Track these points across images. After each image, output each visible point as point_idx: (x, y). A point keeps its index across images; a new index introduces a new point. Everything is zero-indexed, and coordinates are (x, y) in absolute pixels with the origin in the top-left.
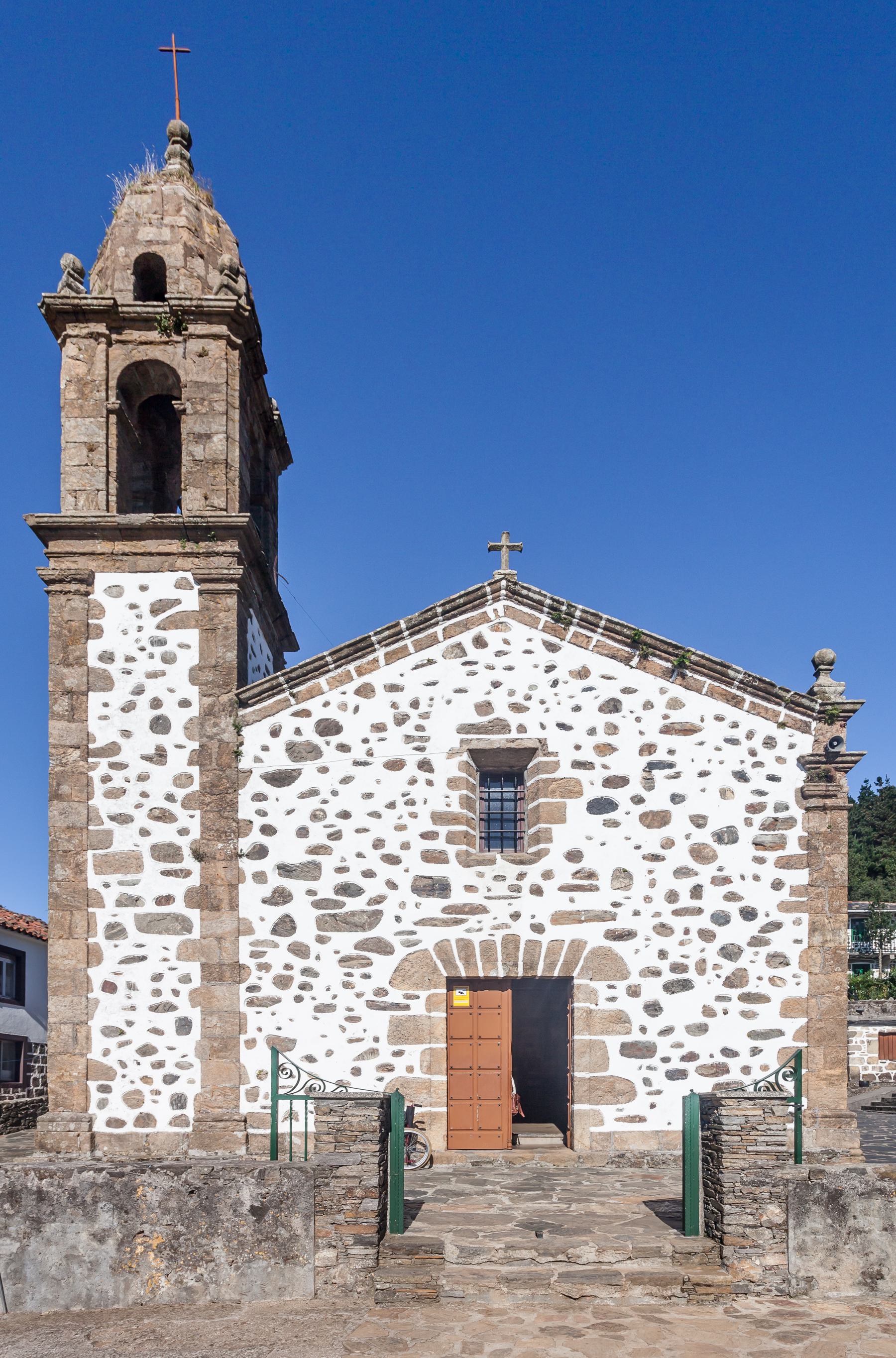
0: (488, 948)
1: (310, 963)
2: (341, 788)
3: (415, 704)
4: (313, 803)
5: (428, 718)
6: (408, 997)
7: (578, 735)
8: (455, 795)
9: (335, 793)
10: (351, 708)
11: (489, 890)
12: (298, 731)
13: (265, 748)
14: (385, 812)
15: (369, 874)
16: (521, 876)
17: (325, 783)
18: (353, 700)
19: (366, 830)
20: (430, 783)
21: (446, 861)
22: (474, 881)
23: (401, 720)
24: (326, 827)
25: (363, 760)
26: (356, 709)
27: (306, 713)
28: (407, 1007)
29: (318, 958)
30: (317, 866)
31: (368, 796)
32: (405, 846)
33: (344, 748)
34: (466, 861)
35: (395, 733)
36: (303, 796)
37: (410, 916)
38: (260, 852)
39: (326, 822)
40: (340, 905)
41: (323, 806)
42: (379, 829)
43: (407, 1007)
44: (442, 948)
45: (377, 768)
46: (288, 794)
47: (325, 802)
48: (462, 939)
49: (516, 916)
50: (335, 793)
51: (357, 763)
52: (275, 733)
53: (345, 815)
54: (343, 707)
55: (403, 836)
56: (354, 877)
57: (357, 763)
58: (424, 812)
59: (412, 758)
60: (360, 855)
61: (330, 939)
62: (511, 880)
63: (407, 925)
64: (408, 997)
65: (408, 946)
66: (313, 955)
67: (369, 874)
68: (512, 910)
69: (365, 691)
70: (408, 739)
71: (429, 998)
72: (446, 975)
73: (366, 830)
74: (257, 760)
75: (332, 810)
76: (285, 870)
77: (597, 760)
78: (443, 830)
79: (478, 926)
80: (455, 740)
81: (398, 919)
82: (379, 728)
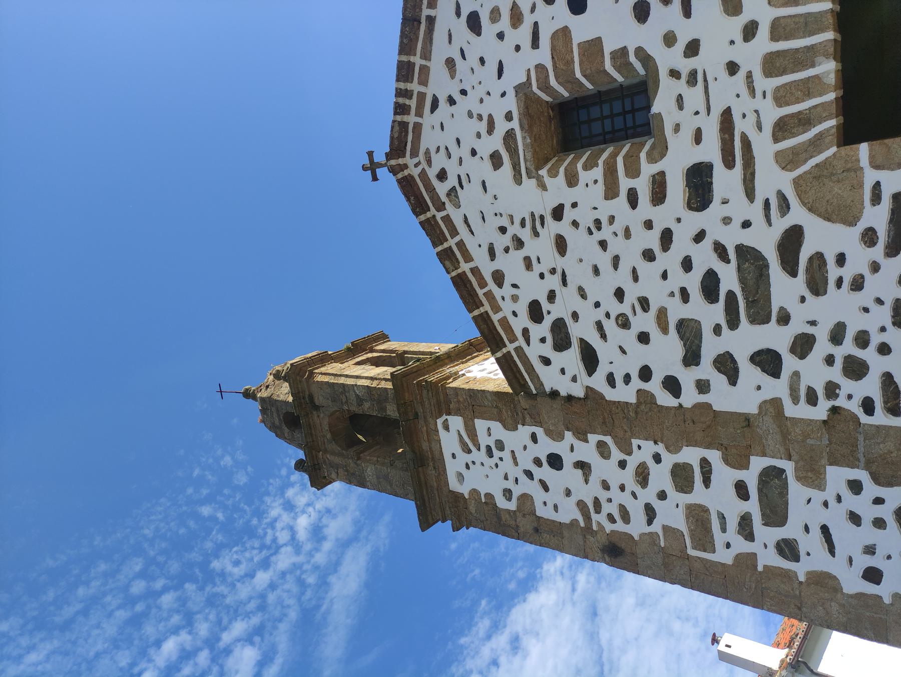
0: (781, 97)
1: (822, 334)
2: (591, 300)
3: (503, 230)
4: (610, 326)
5: (512, 216)
6: (876, 198)
7: (504, 51)
8: (584, 176)
9: (597, 305)
10: (515, 291)
11: (697, 113)
13: (563, 371)
14: (612, 250)
15: (687, 264)
16: (675, 74)
17: (590, 316)
18: (507, 290)
19: (634, 271)
20: (574, 205)
21: (662, 174)
22: (687, 134)
23: (519, 243)
24: (635, 314)
25: (560, 278)
26: (515, 286)
27: (526, 332)
29: (813, 323)
30: (682, 325)
31: (596, 271)
32: (649, 225)
33: (552, 296)
34: (660, 151)
35: (532, 248)
36: (604, 336)
37: (740, 208)
38: (672, 385)
39: (629, 313)
40: (731, 295)
41: (613, 316)
42: (631, 256)
44: (787, 161)
45: (565, 263)
47: (608, 315)
48: (774, 135)
49: (732, 68)
50: (597, 305)
51: (564, 282)
52: (546, 361)
53: (619, 294)
54: (515, 298)
55: (637, 229)
56: (693, 281)
57: (564, 282)
58: (607, 208)
60: (665, 276)
61: (782, 309)
62: (681, 86)
63: (755, 212)
64: (876, 198)
65: (788, 208)
66: (810, 330)
67: (687, 264)
68: (723, 74)
69: (498, 276)
70: (536, 234)
71: (876, 166)
72: (834, 149)
73: (634, 271)
74: (574, 379)
75: (616, 308)
76: (692, 358)
77: (528, 21)
78: (625, 183)
79: (752, 118)
80: (529, 184)
81: (746, 224)
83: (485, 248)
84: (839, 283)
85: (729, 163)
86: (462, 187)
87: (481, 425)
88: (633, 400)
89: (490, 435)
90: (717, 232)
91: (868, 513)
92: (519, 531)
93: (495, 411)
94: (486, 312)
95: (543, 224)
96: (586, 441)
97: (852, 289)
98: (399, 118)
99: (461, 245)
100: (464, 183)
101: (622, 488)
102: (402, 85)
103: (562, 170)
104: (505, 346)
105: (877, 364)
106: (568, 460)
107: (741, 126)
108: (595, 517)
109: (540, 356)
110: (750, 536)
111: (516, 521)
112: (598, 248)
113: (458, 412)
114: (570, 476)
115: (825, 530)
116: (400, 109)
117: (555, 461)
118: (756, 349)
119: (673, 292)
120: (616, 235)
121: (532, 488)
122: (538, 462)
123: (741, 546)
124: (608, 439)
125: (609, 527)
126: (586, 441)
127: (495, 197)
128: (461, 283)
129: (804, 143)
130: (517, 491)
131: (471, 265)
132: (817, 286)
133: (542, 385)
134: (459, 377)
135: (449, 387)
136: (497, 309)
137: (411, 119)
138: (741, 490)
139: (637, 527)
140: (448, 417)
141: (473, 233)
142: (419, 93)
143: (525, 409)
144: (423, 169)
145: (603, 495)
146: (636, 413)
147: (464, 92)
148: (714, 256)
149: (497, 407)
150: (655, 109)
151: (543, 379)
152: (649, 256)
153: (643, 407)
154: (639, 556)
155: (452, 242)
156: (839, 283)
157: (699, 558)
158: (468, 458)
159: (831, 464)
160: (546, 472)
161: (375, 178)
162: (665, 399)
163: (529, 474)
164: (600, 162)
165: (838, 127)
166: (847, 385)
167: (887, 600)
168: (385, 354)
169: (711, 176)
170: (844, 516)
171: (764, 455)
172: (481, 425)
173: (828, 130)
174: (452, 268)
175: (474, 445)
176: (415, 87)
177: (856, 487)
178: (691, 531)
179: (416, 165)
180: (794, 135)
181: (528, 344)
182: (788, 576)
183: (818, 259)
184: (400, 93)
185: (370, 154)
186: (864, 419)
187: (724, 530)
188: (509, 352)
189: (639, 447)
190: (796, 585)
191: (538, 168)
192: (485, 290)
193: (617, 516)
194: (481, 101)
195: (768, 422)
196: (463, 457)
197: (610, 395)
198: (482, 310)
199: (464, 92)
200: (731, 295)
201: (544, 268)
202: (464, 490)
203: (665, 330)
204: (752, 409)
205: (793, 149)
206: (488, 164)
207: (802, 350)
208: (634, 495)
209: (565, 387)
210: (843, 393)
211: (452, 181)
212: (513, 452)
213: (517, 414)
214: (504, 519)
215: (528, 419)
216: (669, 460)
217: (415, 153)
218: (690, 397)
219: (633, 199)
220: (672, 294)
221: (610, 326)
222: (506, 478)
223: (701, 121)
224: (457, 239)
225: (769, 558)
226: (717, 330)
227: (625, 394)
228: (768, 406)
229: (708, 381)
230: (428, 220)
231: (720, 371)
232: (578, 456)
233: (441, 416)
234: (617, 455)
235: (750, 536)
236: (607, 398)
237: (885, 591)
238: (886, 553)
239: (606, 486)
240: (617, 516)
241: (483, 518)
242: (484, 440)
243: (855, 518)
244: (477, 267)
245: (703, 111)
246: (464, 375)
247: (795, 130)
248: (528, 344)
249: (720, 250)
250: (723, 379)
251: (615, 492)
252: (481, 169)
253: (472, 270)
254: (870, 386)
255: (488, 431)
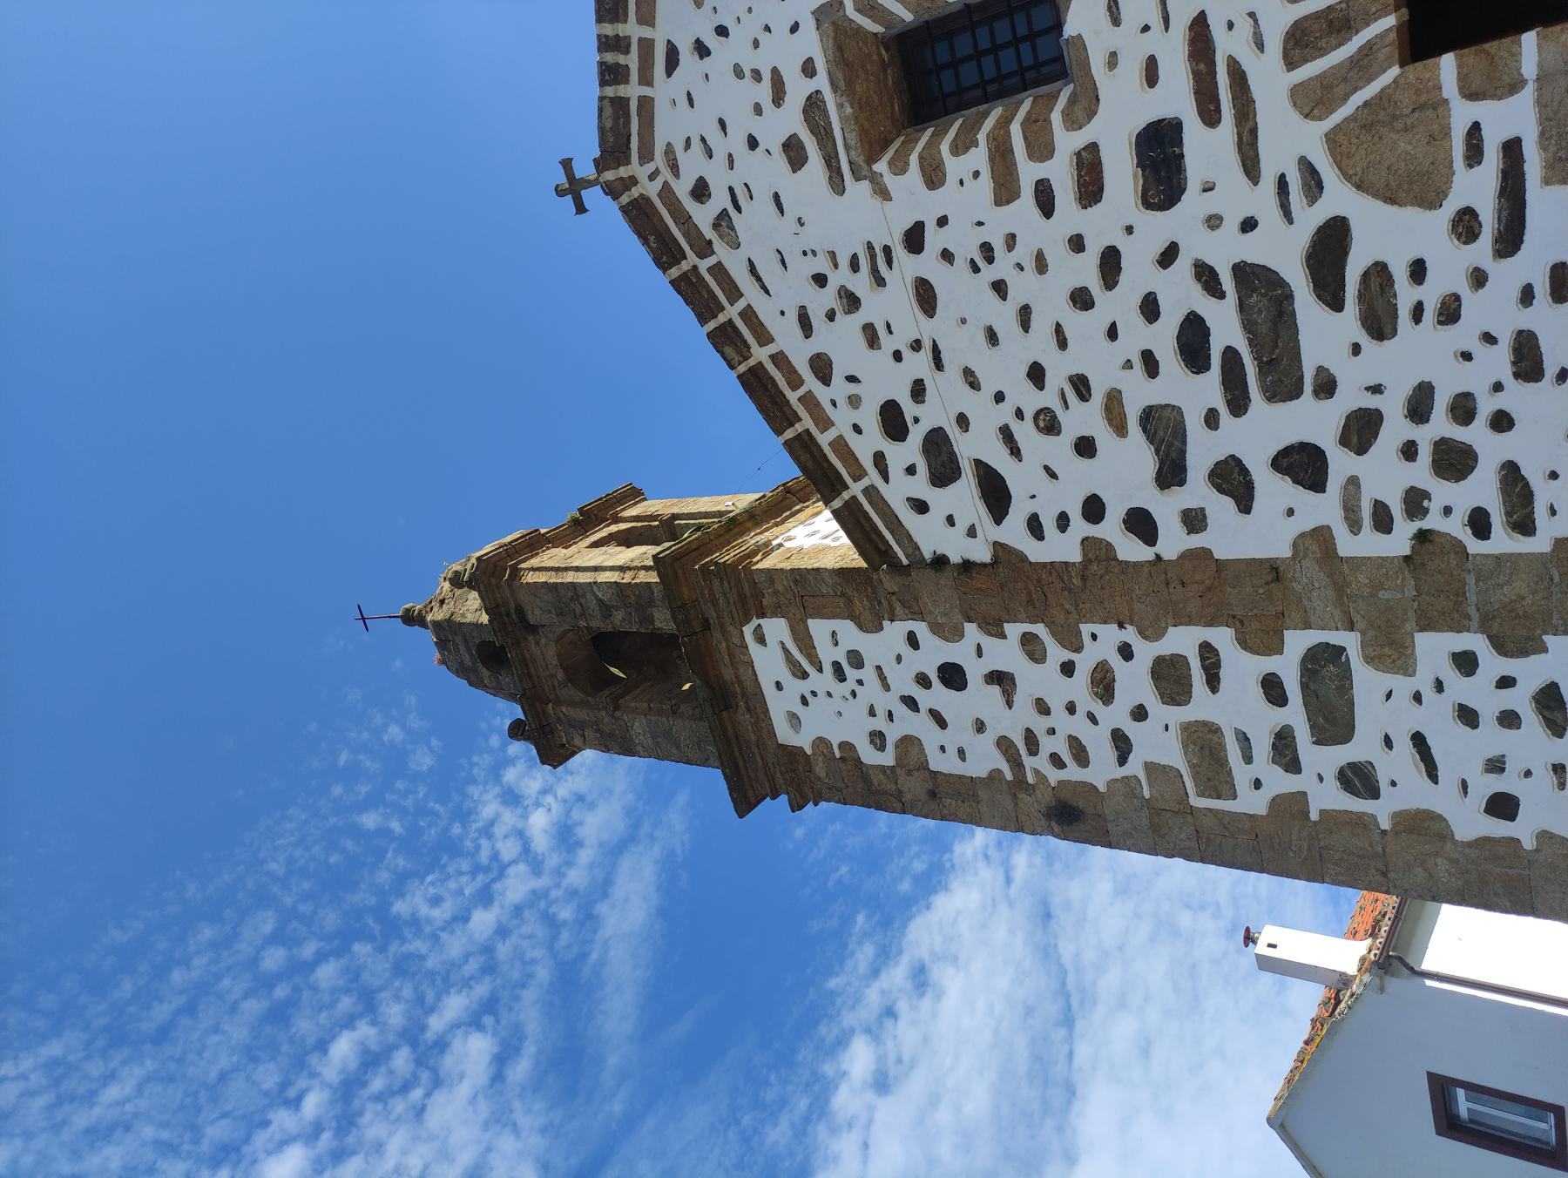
2: (988, 390)
3: (820, 280)
4: (1025, 433)
5: (834, 253)
6: (1474, 153)
8: (955, 166)
9: (999, 397)
10: (853, 389)
11: (1146, 29)
12: (911, 470)
13: (950, 520)
14: (1017, 296)
15: (1150, 308)
17: (987, 418)
19: (1059, 329)
20: (942, 221)
21: (1093, 148)
22: (1131, 68)
25: (930, 355)
26: (852, 379)
27: (879, 459)
28: (1512, 149)
29: (1376, 389)
30: (1150, 417)
31: (992, 337)
32: (1077, 243)
33: (918, 391)
34: (1086, 105)
35: (875, 307)
36: (1015, 452)
38: (1141, 524)
40: (1231, 355)
43: (1512, 149)
44: (1312, 100)
46: (1018, 477)
47: (1019, 414)
50: (999, 397)
51: (938, 364)
52: (921, 507)
53: (1036, 374)
54: (854, 401)
55: (1058, 254)
56: (1163, 338)
57: (938, 364)
58: (1001, 221)
59: (908, 267)
60: (1112, 333)
61: (1321, 370)
63: (1262, 201)
64: (1474, 153)
65: (1320, 186)
66: (1371, 402)
67: (1150, 308)
69: (822, 367)
71: (1471, 94)
72: (1395, 70)
73: (1059, 329)
74: (972, 532)
75: (1032, 400)
76: (1171, 473)
78: (1029, 172)
79: (1244, 28)
80: (859, 190)
81: (1249, 225)
82: (871, 336)
83: (792, 316)
84: (1418, 313)
85: (1210, 116)
86: (738, 208)
87: (819, 629)
88: (1075, 556)
89: (837, 644)
90: (1199, 245)
91: (1489, 703)
92: (903, 800)
93: (841, 602)
94: (807, 431)
95: (889, 262)
96: (1003, 636)
97: (1440, 323)
98: (610, 91)
99: (749, 314)
100: (742, 202)
101: (1071, 708)
102: (608, 29)
103: (914, 159)
104: (847, 488)
105: (1491, 449)
106: (975, 671)
107: (1227, 45)
108: (1029, 762)
109: (908, 499)
110: (1293, 766)
111: (896, 783)
112: (991, 295)
113: (777, 611)
114: (980, 698)
115: (1419, 740)
116: (611, 74)
117: (953, 676)
118: (1281, 446)
119: (1129, 361)
120: (1022, 269)
121: (919, 726)
122: (923, 681)
123: (1280, 782)
124: (1040, 629)
125: (1054, 776)
126: (1003, 636)
127: (800, 222)
128: (758, 385)
129: (1340, 65)
130: (893, 734)
131: (771, 349)
132: (1379, 324)
133: (917, 548)
134: (772, 550)
135: (757, 569)
136: (825, 423)
137: (632, 91)
138: (1273, 689)
139: (1102, 771)
140: (761, 621)
141: (767, 292)
142: (641, 40)
143: (893, 594)
144: (666, 183)
145: (1039, 724)
146: (1084, 579)
147: (722, 31)
148: (1197, 289)
149: (843, 594)
150: (1069, 30)
151: (917, 538)
152: (1082, 299)
153: (1094, 567)
154: (1108, 818)
155: (732, 312)
156: (1418, 313)
157: (1210, 810)
158: (804, 687)
159: (1421, 630)
160: (939, 696)
161: (581, 209)
162: (1131, 549)
163: (911, 703)
164: (982, 137)
165: (1399, 28)
166: (1442, 492)
167: (1528, 844)
168: (640, 524)
169: (1180, 143)
170: (1449, 713)
171: (1307, 626)
172: (819, 629)
173: (1381, 36)
174: (737, 358)
175: (812, 663)
176: (631, 29)
177: (1466, 663)
178: (1193, 767)
179: (652, 177)
180: (1322, 52)
181: (886, 480)
182: (1363, 823)
183: (1379, 274)
184: (606, 44)
185: (567, 164)
186: (1475, 546)
187: (1248, 759)
188: (854, 498)
189: (1094, 637)
190: (1376, 837)
191: (872, 159)
192: (801, 392)
193: (1066, 756)
194: (756, 44)
195: (1311, 572)
196: (795, 687)
197: (1037, 552)
198: (799, 428)
199: (722, 31)
200: (1231, 355)
201: (900, 341)
202: (803, 740)
203: (1120, 429)
204: (1278, 547)
205: (1321, 77)
206: (780, 161)
207: (1360, 438)
208: (1092, 718)
209: (957, 548)
210: (1435, 506)
211: (719, 200)
212: (879, 668)
213: (880, 603)
214: (875, 782)
215: (899, 609)
216: (1146, 652)
217: (646, 155)
218: (1173, 542)
219: (1045, 200)
220: (1128, 365)
221: (1025, 433)
222: (872, 713)
223: (1155, 43)
224: (741, 305)
225: (1327, 798)
226: (1212, 420)
227: (1062, 548)
228: (1308, 542)
229: (1203, 510)
230: (684, 276)
231: (1221, 491)
232: (992, 662)
233: (748, 621)
234: (1057, 654)
235: (1293, 766)
236: (1032, 559)
237: (1523, 830)
238: (1523, 767)
239: (1043, 708)
240: (1066, 756)
241: (840, 784)
242: (828, 654)
243: (1468, 716)
244: (781, 352)
245: (1156, 22)
246: (780, 545)
247: (1322, 44)
248: (886, 480)
249: (1206, 276)
250: (1228, 503)
251: (1059, 717)
252: (768, 171)
253: (773, 358)
254: (1482, 489)
255: (833, 636)
